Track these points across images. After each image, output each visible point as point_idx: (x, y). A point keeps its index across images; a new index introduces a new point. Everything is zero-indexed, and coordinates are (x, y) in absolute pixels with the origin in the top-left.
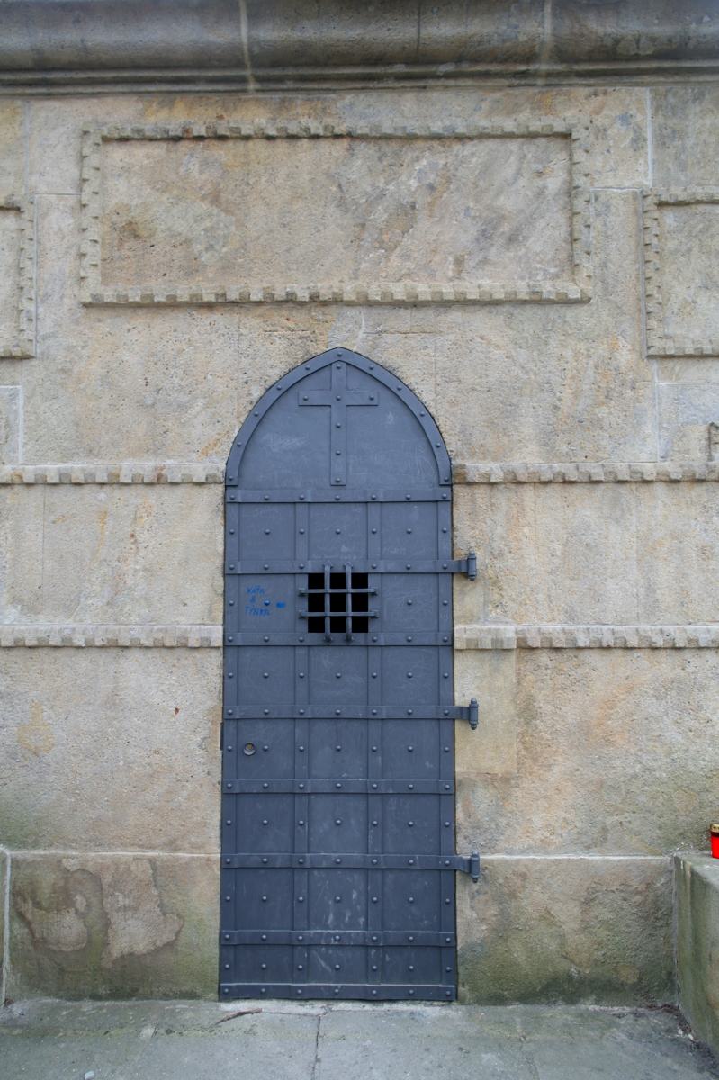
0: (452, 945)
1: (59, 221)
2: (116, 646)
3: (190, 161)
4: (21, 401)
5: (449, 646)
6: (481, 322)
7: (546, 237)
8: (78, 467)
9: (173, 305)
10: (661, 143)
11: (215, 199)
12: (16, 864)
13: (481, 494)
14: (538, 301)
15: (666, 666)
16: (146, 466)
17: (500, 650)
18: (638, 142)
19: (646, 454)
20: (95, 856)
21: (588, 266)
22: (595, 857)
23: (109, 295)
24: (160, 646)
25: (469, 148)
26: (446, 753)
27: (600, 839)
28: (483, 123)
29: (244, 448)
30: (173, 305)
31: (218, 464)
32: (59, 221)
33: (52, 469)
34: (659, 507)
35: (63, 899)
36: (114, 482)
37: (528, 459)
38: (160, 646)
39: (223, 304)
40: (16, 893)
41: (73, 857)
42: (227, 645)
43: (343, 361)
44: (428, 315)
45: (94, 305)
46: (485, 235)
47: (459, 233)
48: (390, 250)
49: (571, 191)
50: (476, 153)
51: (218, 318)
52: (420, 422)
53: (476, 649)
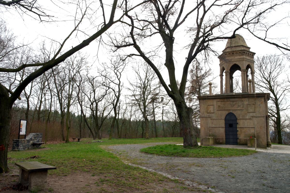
0: (237, 142)
1: (216, 106)
2: (219, 127)
3: (223, 103)
4: (214, 115)
5: (237, 127)
6: (238, 111)
7: (242, 106)
8: (217, 118)
9: (222, 110)
10: (248, 101)
11: (224, 104)
12: (215, 138)
13: (238, 120)
14: (241, 110)
15: (249, 129)
16: (221, 118)
17: (239, 128)
18: (247, 101)
19: (247, 117)
20: (219, 137)
21: (244, 108)
22: (245, 138)
23: (218, 110)
24: (222, 127)
26: (237, 133)
27: (245, 137)
28: (238, 100)
29: (226, 117)
30: (222, 110)
31: (224, 118)
33: (216, 118)
34: (248, 120)
35: (217, 139)
36: (219, 119)
37: (241, 118)
38: (222, 127)
39: (224, 110)
40: (215, 139)
41: (218, 137)
42: (225, 127)
43: (231, 113)
44: (235, 111)
45: (218, 110)
46: (238, 106)
47: (237, 106)
48: (233, 107)
49: (243, 104)
50: (238, 102)
51: (224, 111)
52: (235, 116)
53: (238, 128)
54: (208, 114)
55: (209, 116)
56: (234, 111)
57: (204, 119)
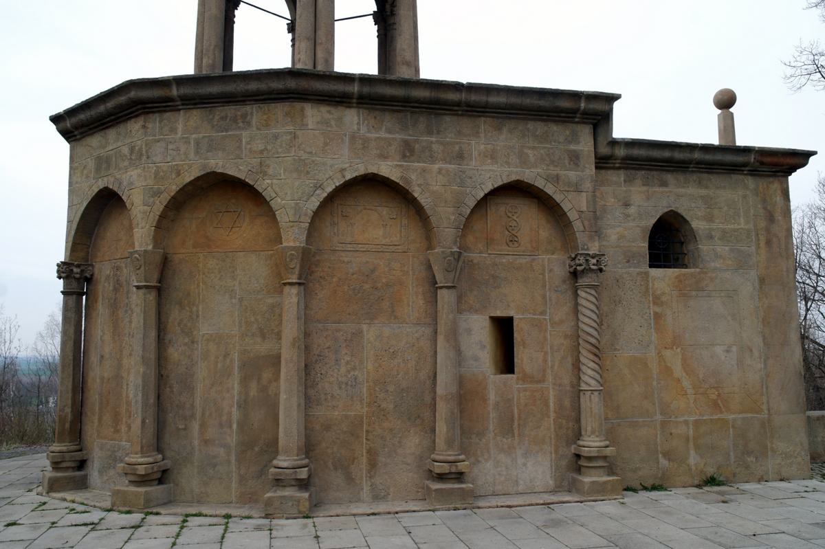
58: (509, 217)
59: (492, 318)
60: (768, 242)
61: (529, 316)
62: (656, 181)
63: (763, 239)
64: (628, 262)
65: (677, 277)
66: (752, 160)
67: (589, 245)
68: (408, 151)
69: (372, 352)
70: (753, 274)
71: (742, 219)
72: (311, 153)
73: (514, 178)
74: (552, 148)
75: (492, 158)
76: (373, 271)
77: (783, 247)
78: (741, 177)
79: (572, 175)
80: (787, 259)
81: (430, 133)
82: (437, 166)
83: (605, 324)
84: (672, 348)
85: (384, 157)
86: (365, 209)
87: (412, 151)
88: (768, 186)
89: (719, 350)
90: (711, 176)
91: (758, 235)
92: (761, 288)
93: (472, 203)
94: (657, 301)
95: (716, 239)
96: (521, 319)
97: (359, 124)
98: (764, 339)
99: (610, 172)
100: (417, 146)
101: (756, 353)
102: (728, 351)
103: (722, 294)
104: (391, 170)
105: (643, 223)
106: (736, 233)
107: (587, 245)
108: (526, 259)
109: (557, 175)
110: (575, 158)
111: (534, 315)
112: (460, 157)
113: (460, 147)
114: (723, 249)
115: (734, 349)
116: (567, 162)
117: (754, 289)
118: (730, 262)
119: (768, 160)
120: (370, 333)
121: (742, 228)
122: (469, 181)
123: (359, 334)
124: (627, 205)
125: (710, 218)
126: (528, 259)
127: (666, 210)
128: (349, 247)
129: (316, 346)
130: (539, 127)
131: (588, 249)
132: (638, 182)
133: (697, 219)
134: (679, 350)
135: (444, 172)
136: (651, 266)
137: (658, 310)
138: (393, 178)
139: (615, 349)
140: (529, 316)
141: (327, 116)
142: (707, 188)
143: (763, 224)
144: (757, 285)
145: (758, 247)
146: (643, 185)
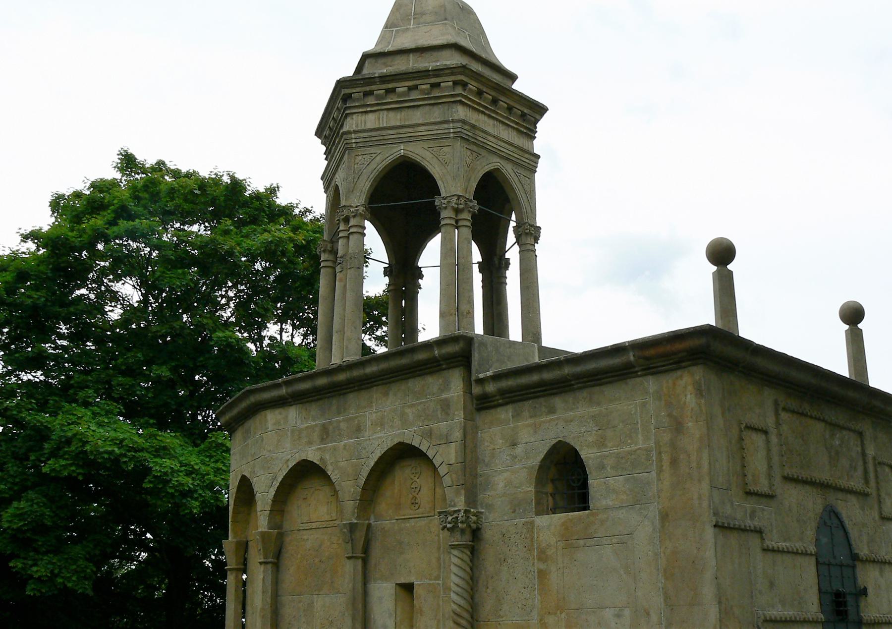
1: (774, 439)
6: (853, 499)
25: (844, 432)
32: (774, 439)
51: (808, 488)
54: (750, 505)
55: (756, 523)
56: (840, 495)
57: (734, 539)
58: (412, 479)
59: (396, 584)
60: (674, 462)
61: (427, 581)
62: (544, 409)
63: (666, 457)
64: (514, 512)
65: (563, 524)
66: (632, 358)
67: (456, 500)
68: (325, 434)
69: (319, 621)
70: (653, 511)
71: (640, 436)
72: (270, 451)
73: (396, 441)
74: (427, 402)
75: (382, 425)
76: (320, 546)
77: (694, 465)
78: (638, 380)
79: (442, 426)
80: (699, 481)
81: (339, 413)
82: (343, 443)
83: (490, 588)
84: (555, 614)
85: (310, 443)
86: (316, 490)
87: (327, 433)
88: (674, 384)
89: (608, 614)
90: (603, 388)
91: (660, 453)
92: (663, 527)
93: (365, 473)
94: (543, 556)
95: (608, 469)
96: (419, 585)
97: (296, 417)
98: (667, 597)
99: (499, 410)
100: (331, 428)
101: (654, 618)
102: (618, 616)
103: (614, 540)
104: (315, 453)
105: (530, 463)
106: (633, 457)
107: (454, 501)
108: (424, 521)
109: (431, 431)
110: (446, 406)
111: (430, 580)
112: (359, 429)
113: (359, 421)
114: (617, 482)
115: (627, 612)
116: (439, 412)
117: (654, 529)
118: (624, 497)
119: (652, 352)
120: (319, 602)
121: (639, 449)
122: (364, 451)
123: (311, 605)
124: (514, 444)
125: (601, 443)
126: (426, 520)
127: (554, 442)
128: (306, 526)
129: (287, 615)
130: (416, 384)
131: (455, 506)
132: (526, 414)
133: (587, 446)
134: (563, 615)
135: (347, 447)
136: (538, 514)
137: (542, 566)
138: (315, 461)
139: (500, 616)
140: (427, 581)
141: (279, 417)
142: (598, 404)
143: (666, 437)
144: (657, 522)
145: (660, 470)
146: (531, 417)
